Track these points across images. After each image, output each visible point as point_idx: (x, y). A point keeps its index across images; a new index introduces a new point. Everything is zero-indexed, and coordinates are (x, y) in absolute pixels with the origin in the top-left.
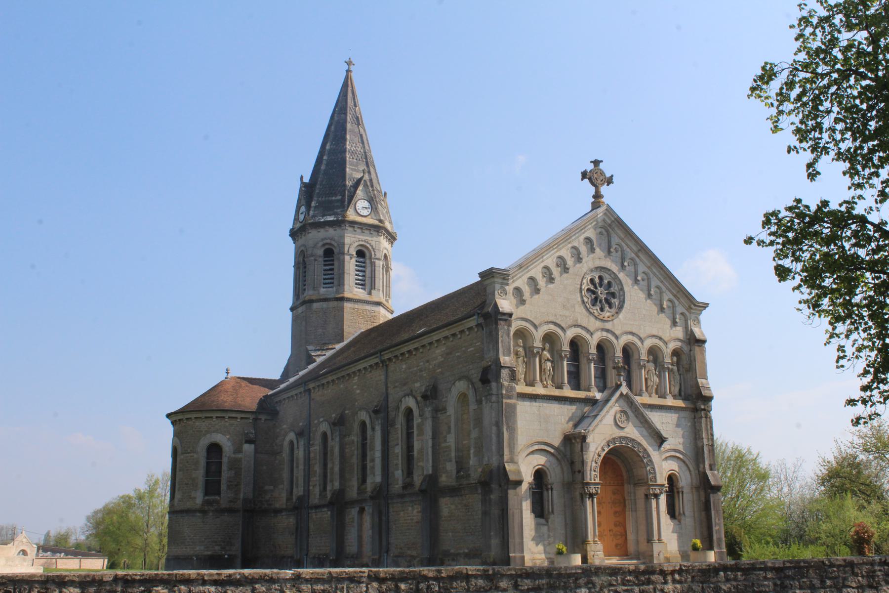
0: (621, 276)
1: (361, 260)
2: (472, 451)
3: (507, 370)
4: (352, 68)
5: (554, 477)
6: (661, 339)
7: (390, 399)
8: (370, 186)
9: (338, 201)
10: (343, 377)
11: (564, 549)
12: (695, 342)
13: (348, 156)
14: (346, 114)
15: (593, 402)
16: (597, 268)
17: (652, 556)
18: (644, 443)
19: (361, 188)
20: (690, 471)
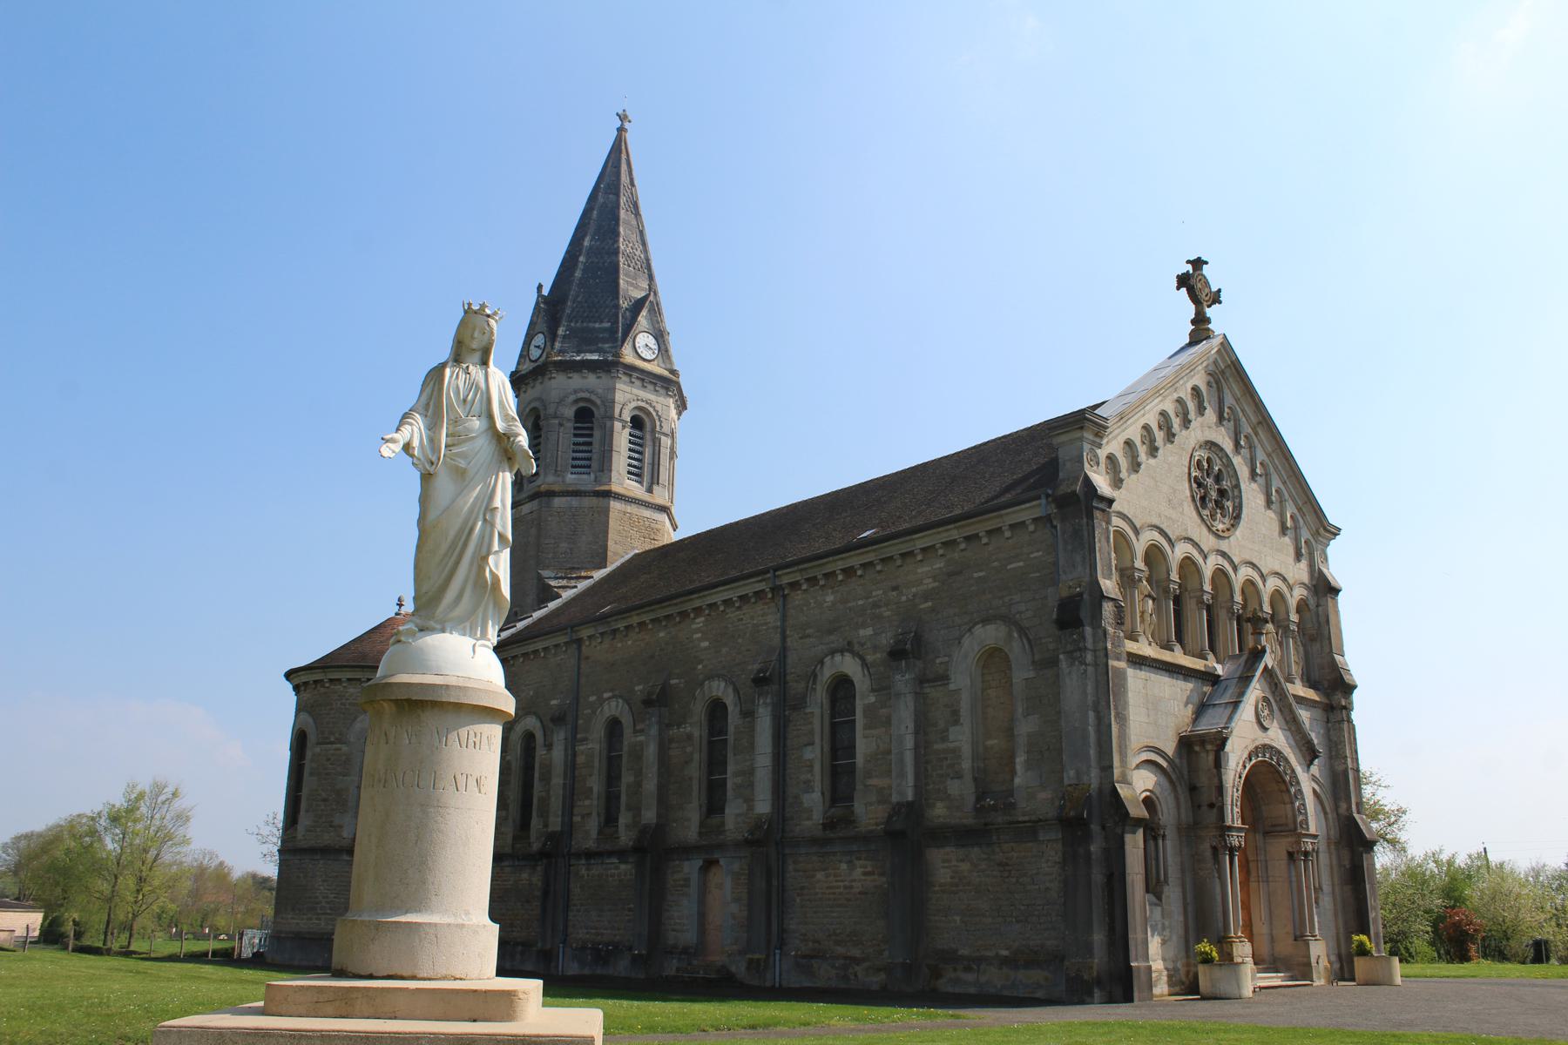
0: (1237, 461)
1: (638, 433)
2: (1020, 760)
3: (1111, 604)
4: (627, 125)
5: (1168, 815)
6: (1284, 580)
7: (792, 658)
8: (656, 311)
9: (605, 330)
10: (668, 617)
11: (1215, 954)
12: (1324, 589)
13: (622, 260)
14: (618, 196)
15: (1211, 678)
16: (1207, 442)
17: (1309, 964)
19: (644, 313)
20: (1325, 813)
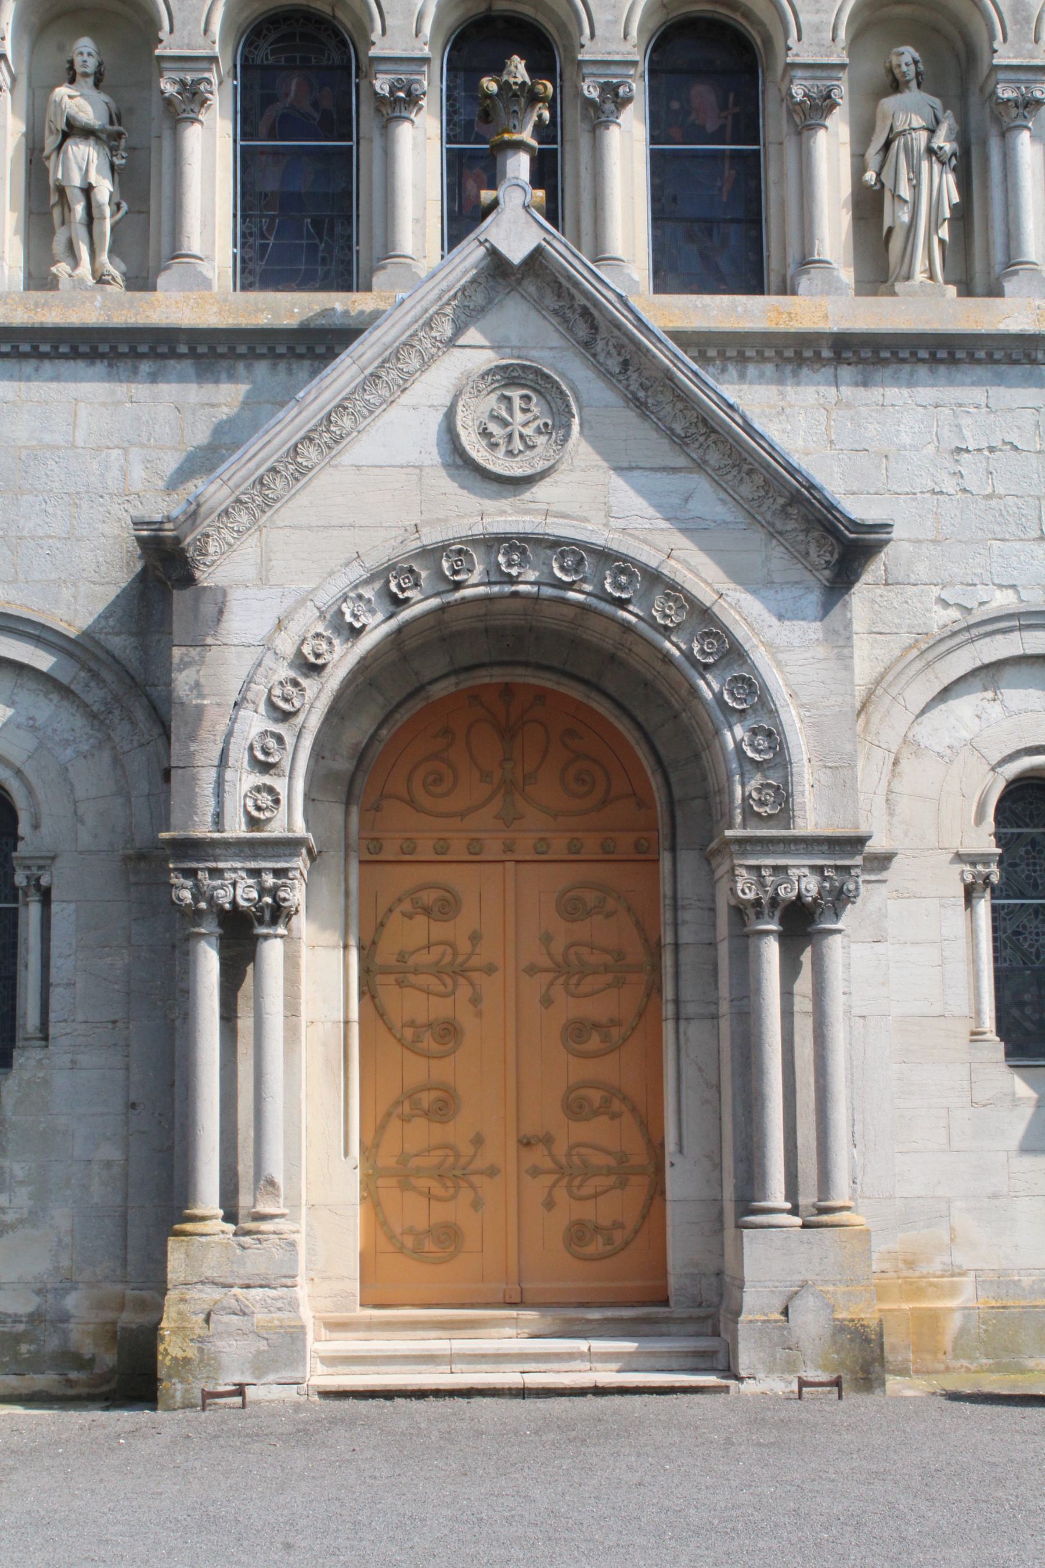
18: (699, 573)
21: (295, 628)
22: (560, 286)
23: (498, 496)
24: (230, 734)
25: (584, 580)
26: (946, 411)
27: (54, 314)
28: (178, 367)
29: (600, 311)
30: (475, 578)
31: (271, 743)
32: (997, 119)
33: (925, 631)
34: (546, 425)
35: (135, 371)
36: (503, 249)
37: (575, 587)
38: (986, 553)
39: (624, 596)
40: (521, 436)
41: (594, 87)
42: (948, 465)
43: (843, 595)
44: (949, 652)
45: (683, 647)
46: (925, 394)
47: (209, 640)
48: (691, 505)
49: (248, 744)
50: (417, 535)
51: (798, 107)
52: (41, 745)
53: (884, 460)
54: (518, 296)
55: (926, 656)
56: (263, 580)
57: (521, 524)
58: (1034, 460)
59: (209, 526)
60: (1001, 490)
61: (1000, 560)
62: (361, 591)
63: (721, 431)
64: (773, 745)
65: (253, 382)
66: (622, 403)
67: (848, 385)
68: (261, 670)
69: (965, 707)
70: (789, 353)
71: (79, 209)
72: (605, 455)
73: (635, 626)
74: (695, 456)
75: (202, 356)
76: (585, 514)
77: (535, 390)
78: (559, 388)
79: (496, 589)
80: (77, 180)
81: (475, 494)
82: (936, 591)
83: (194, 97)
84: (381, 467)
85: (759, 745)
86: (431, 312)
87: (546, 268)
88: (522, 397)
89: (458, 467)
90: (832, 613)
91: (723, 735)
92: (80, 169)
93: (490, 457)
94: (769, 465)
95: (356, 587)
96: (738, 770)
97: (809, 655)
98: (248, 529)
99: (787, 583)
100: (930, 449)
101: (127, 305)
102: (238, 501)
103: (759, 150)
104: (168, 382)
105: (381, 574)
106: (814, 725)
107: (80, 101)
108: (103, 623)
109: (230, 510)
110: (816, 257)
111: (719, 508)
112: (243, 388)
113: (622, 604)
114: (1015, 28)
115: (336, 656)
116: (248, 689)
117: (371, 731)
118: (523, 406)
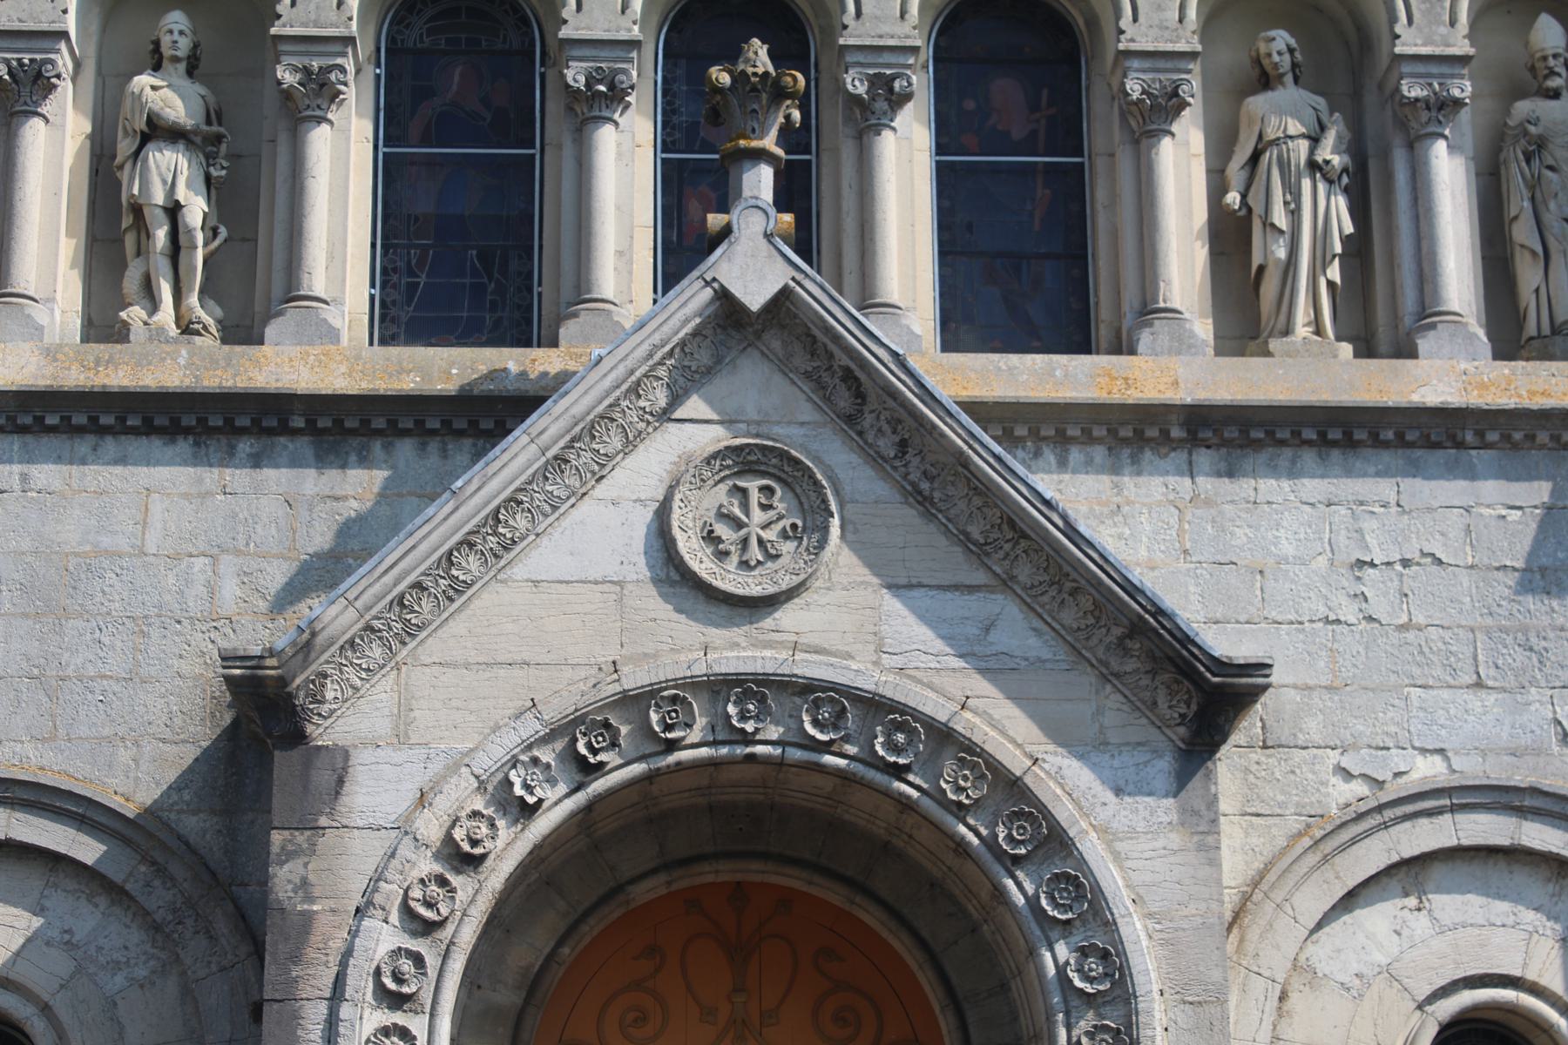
18: (1005, 729)
21: (444, 804)
22: (814, 340)
23: (729, 623)
24: (348, 953)
25: (846, 739)
26: (1343, 511)
27: (121, 374)
28: (291, 446)
29: (869, 375)
30: (695, 735)
31: (407, 966)
32: (1402, 125)
33: (1320, 812)
34: (794, 526)
35: (231, 451)
36: (737, 291)
37: (835, 748)
38: (1402, 704)
39: (901, 761)
40: (761, 542)
41: (861, 81)
42: (1346, 584)
43: (1204, 761)
44: (1354, 841)
45: (984, 832)
46: (1313, 487)
47: (323, 821)
48: (992, 637)
49: (373, 967)
50: (615, 676)
51: (1134, 108)
52: (79, 969)
53: (1258, 577)
54: (756, 354)
55: (1321, 847)
56: (401, 738)
57: (760, 661)
58: (1465, 578)
59: (328, 662)
60: (1419, 618)
61: (1421, 714)
62: (536, 753)
63: (1033, 535)
64: (1109, 971)
65: (392, 467)
66: (898, 497)
67: (1207, 475)
68: (395, 863)
69: (1379, 920)
70: (1126, 432)
71: (161, 235)
72: (873, 566)
73: (916, 802)
74: (998, 570)
75: (324, 431)
76: (847, 648)
77: (779, 479)
78: (812, 476)
79: (724, 751)
80: (159, 197)
81: (696, 620)
82: (1333, 757)
83: (321, 91)
84: (567, 582)
85: (1091, 970)
86: (638, 374)
87: (796, 316)
88: (762, 489)
89: (673, 584)
90: (1190, 786)
91: (1040, 956)
92: (164, 182)
93: (716, 570)
94: (1100, 582)
95: (530, 747)
96: (1061, 1006)
97: (1159, 844)
98: (382, 667)
99: (1128, 744)
100: (1322, 562)
101: (222, 363)
102: (369, 628)
103: (1082, 164)
104: (277, 466)
105: (565, 729)
106: (1165, 943)
107: (167, 93)
108: (175, 797)
109: (358, 640)
110: (1162, 305)
111: (1033, 641)
112: (380, 475)
113: (899, 772)
114: (1423, 7)
115: (500, 843)
116: (375, 890)
117: (547, 950)
118: (763, 501)
